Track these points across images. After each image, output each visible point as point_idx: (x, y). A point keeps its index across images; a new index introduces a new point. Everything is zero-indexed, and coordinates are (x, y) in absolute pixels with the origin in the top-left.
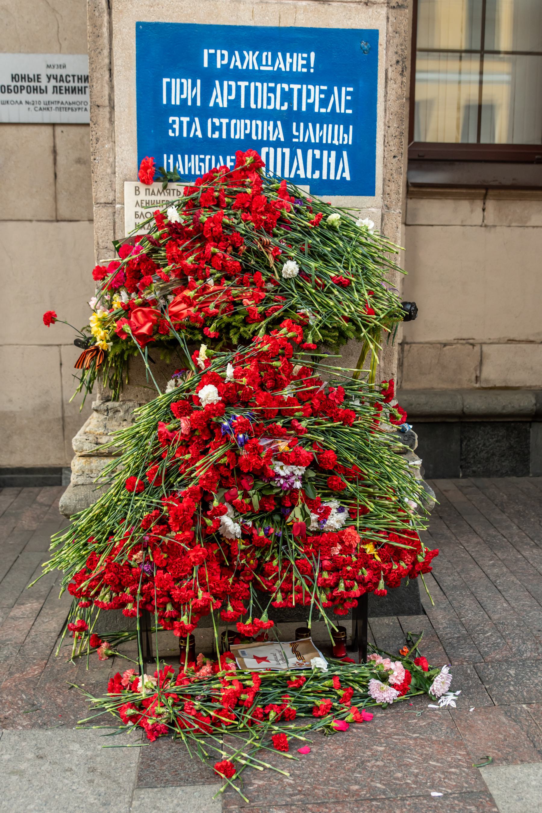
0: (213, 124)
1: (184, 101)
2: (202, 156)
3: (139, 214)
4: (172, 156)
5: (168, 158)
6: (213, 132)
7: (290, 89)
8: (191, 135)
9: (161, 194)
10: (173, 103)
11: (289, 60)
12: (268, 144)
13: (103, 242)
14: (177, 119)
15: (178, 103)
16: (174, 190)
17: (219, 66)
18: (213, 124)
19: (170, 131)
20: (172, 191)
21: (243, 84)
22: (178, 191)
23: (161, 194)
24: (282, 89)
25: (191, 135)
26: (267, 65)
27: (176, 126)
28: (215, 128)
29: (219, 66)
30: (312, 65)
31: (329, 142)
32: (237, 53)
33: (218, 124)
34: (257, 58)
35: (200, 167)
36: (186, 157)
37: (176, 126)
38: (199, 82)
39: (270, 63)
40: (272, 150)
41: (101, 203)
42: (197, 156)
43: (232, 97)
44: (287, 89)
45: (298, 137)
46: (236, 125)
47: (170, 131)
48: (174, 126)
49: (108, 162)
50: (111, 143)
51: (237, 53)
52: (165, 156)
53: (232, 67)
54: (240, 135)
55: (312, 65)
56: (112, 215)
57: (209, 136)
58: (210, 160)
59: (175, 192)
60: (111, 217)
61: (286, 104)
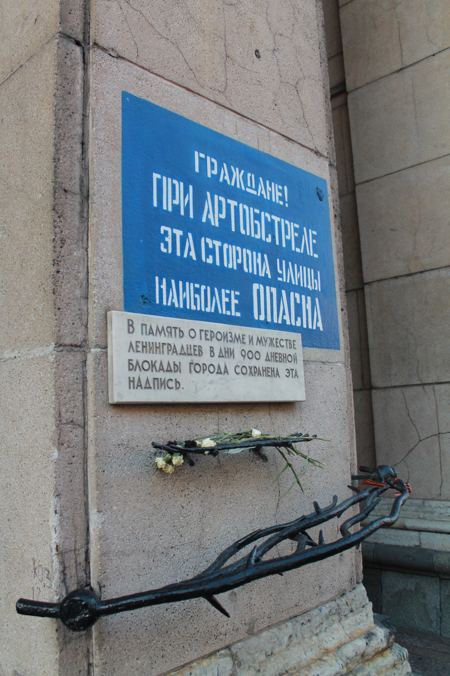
0: (207, 245)
1: (176, 208)
2: (197, 286)
3: (134, 363)
4: (164, 280)
5: (161, 283)
6: (207, 257)
7: (272, 220)
8: (185, 256)
9: (160, 333)
10: (165, 208)
11: (268, 188)
12: (257, 279)
13: (67, 411)
14: (169, 229)
15: (170, 209)
16: (175, 328)
17: (209, 176)
18: (207, 245)
19: (162, 245)
20: (173, 330)
21: (233, 203)
22: (180, 331)
23: (160, 333)
24: (266, 218)
25: (185, 256)
26: (251, 188)
27: (169, 240)
28: (210, 252)
29: (209, 176)
30: (286, 200)
31: (305, 286)
32: (225, 165)
33: (211, 246)
34: (243, 177)
35: (195, 299)
36: (181, 283)
37: (169, 240)
38: (191, 187)
39: (254, 187)
40: (262, 287)
41: (65, 345)
42: (192, 284)
43: (223, 216)
44: (269, 220)
45: (281, 276)
46: (228, 250)
47: (162, 245)
48: (167, 239)
49: (76, 278)
50: (81, 250)
51: (225, 165)
52: (157, 278)
53: (221, 180)
54: (232, 265)
55: (286, 200)
56: (80, 365)
57: (204, 259)
58: (206, 291)
59: (177, 331)
60: (79, 370)
61: (270, 236)
